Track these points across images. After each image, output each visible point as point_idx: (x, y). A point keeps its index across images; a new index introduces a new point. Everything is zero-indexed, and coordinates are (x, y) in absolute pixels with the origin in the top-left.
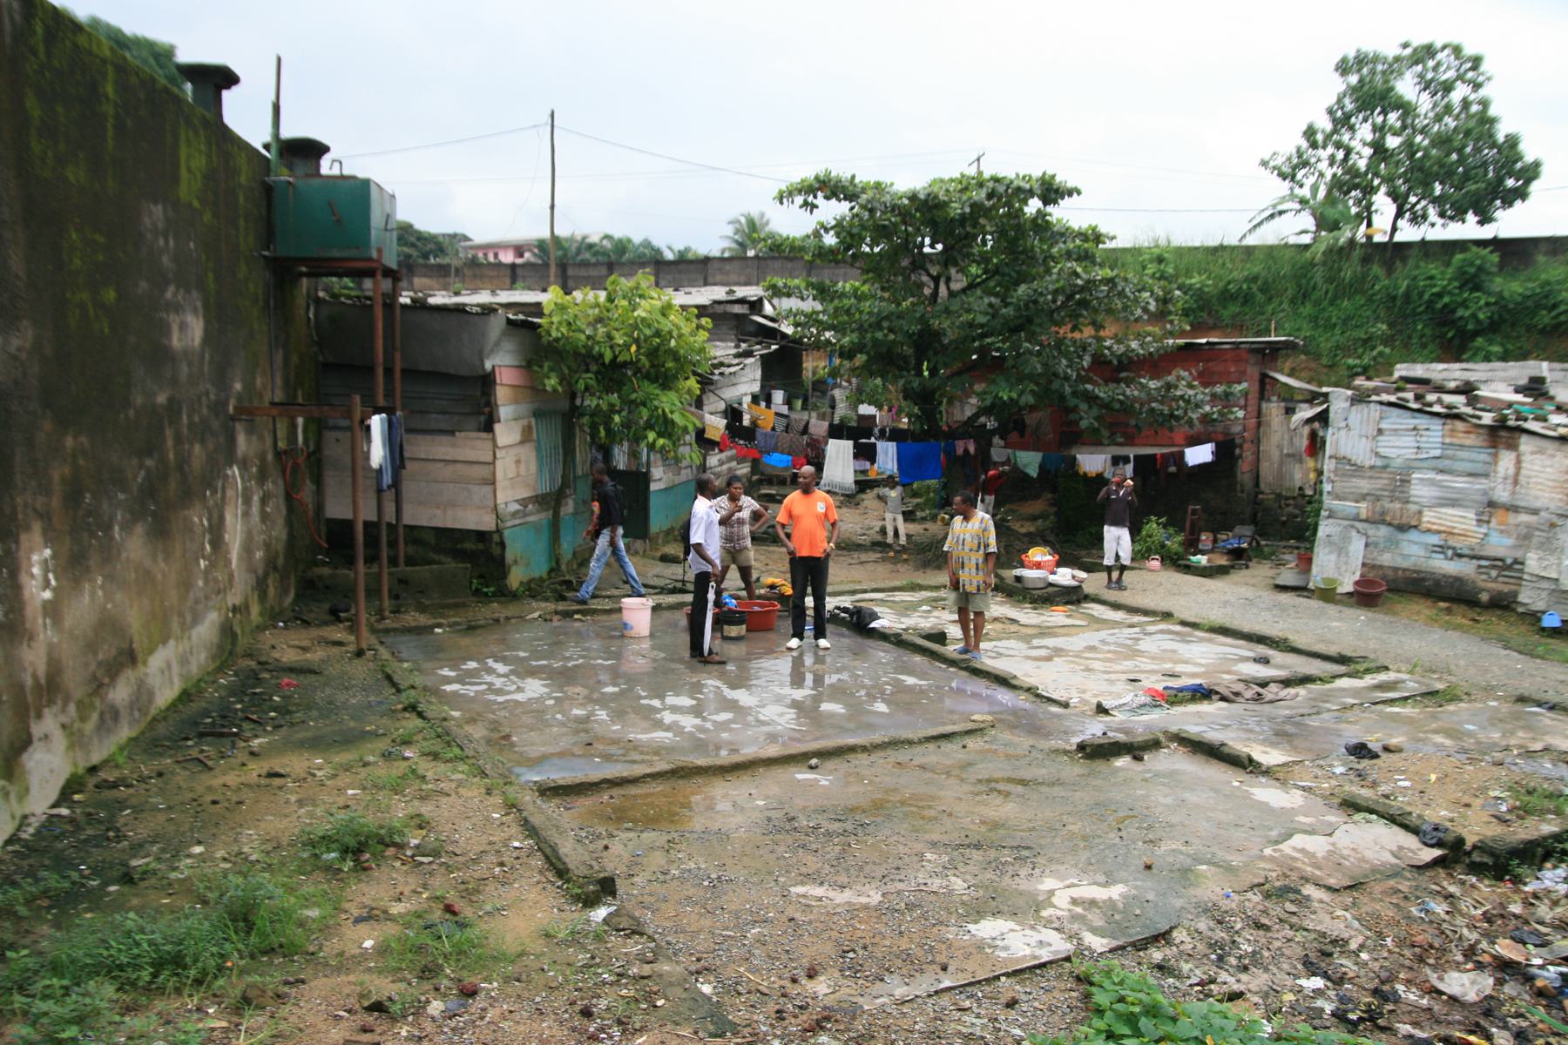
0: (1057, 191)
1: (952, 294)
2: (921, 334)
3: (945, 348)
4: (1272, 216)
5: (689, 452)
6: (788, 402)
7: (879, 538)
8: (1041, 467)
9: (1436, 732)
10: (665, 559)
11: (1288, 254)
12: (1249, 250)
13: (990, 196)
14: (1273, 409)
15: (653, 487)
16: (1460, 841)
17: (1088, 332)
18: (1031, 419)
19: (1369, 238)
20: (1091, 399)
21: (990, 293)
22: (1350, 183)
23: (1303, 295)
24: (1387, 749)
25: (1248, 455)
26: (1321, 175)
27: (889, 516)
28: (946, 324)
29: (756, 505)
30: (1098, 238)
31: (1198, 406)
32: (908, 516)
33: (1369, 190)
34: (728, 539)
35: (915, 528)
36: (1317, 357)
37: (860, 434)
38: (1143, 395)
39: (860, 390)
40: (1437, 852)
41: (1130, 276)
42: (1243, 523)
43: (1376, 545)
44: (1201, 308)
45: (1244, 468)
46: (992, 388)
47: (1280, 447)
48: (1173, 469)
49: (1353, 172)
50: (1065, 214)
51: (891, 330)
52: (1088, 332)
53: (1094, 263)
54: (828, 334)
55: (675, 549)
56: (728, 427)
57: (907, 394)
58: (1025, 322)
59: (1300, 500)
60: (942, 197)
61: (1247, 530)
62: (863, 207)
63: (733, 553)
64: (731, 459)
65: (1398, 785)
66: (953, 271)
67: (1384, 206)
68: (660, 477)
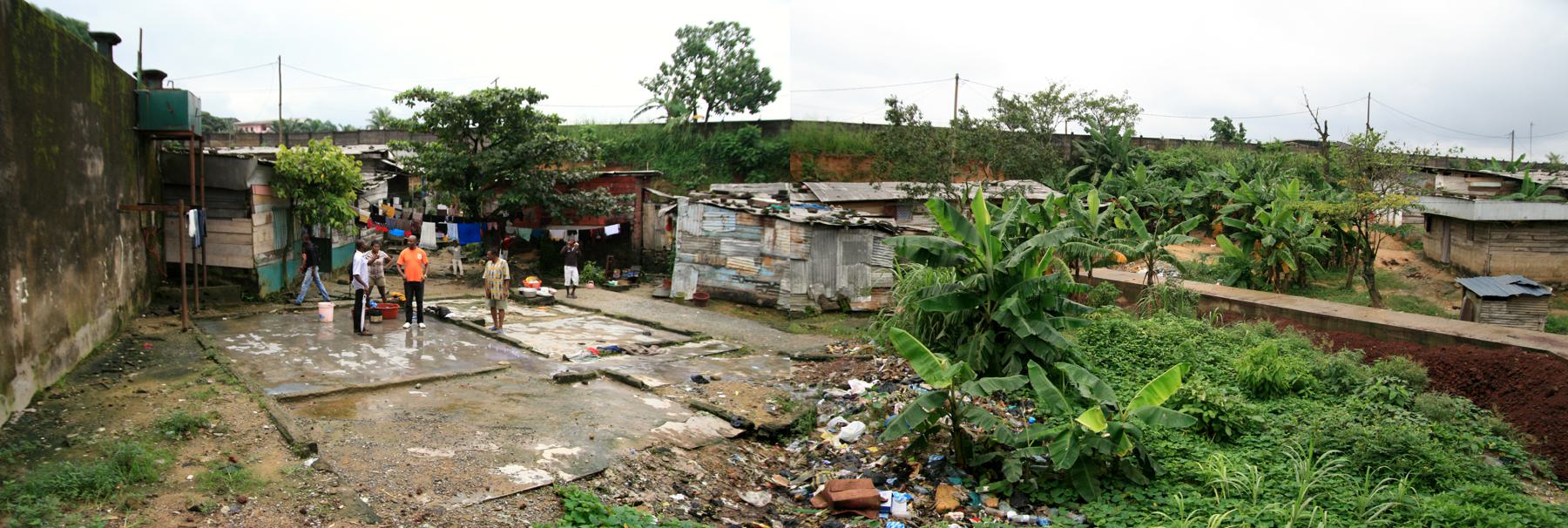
0: (536, 96)
1: (484, 149)
2: (469, 169)
3: (481, 176)
4: (646, 109)
5: (352, 229)
6: (402, 203)
7: (449, 272)
8: (532, 236)
9: (737, 370)
10: (340, 282)
11: (654, 128)
12: (634, 127)
13: (502, 99)
14: (649, 207)
15: (334, 246)
16: (752, 425)
17: (554, 168)
18: (526, 212)
19: (695, 120)
20: (556, 202)
21: (503, 148)
22: (684, 92)
23: (663, 149)
24: (712, 379)
25: (637, 230)
26: (670, 88)
27: (454, 261)
28: (481, 164)
29: (387, 256)
30: (557, 120)
31: (611, 205)
32: (464, 261)
33: (695, 96)
34: (372, 272)
35: (468, 267)
36: (671, 180)
37: (439, 220)
38: (583, 200)
39: (438, 197)
40: (740, 431)
41: (574, 139)
42: (635, 264)
43: (704, 275)
44: (611, 156)
45: (635, 236)
46: (506, 196)
47: (653, 226)
48: (599, 237)
49: (686, 87)
50: (540, 108)
51: (453, 167)
52: (554, 168)
53: (556, 133)
54: (421, 169)
55: (345, 278)
56: (371, 216)
57: (462, 199)
58: (521, 163)
59: (664, 254)
60: (478, 100)
61: (638, 268)
62: (438, 105)
63: (375, 279)
64: (373, 232)
65: (720, 397)
66: (484, 137)
67: (702, 104)
68: (337, 242)
